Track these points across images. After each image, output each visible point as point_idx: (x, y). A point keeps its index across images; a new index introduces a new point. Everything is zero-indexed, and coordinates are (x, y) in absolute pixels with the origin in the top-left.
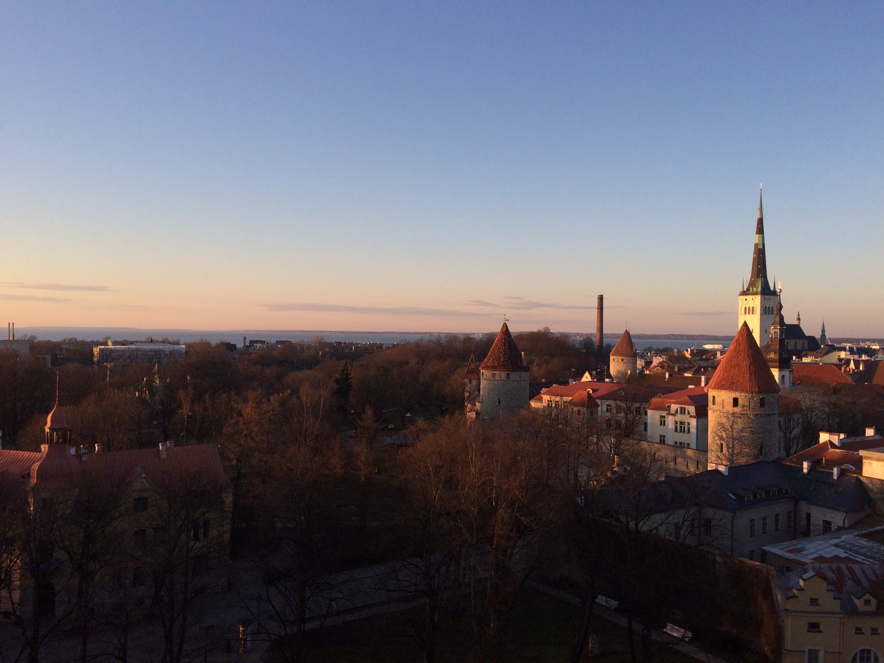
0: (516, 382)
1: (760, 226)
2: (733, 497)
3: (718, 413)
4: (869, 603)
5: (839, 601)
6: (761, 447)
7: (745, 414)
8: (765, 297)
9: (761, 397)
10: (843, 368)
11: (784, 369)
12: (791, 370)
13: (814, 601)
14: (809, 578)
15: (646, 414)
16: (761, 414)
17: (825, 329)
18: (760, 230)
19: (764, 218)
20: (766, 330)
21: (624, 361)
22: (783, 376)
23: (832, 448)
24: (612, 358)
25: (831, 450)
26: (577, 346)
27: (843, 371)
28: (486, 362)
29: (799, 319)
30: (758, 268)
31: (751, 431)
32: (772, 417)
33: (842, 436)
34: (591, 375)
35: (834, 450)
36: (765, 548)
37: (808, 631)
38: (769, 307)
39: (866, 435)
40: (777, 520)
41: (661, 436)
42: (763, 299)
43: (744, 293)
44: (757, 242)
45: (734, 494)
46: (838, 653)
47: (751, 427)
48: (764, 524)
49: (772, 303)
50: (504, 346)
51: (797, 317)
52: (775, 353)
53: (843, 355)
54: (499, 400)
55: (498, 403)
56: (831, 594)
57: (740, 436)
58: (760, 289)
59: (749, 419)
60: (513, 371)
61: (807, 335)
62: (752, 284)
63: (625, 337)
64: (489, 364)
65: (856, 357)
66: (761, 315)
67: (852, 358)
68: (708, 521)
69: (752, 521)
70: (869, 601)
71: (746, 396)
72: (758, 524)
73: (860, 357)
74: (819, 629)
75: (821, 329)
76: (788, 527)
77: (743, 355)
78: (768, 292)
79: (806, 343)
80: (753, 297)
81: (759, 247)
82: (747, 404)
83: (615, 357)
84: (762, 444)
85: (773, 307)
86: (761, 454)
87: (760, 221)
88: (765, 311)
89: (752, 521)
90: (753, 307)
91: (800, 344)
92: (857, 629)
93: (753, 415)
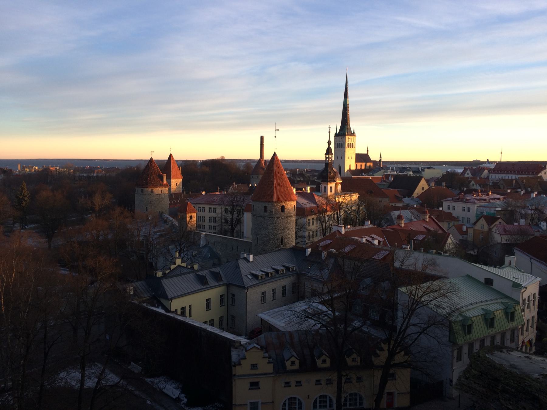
1: (346, 93)
2: (250, 278)
3: (256, 217)
4: (294, 364)
5: (272, 365)
6: (282, 239)
7: (271, 217)
9: (282, 205)
11: (331, 182)
12: (336, 183)
13: (254, 366)
14: (249, 350)
15: (243, 214)
17: (382, 156)
18: (346, 96)
20: (349, 157)
21: (259, 178)
22: (331, 187)
24: (251, 176)
26: (242, 168)
29: (368, 151)
34: (235, 188)
37: (249, 389)
38: (351, 144)
40: (284, 291)
46: (270, 402)
55: (146, 210)
56: (266, 360)
57: (268, 232)
59: (274, 220)
68: (233, 295)
69: (264, 293)
70: (294, 362)
71: (272, 205)
72: (269, 296)
74: (258, 386)
76: (293, 294)
80: (342, 137)
85: (353, 144)
86: (282, 244)
89: (264, 293)
90: (342, 143)
92: (286, 383)
93: (276, 217)
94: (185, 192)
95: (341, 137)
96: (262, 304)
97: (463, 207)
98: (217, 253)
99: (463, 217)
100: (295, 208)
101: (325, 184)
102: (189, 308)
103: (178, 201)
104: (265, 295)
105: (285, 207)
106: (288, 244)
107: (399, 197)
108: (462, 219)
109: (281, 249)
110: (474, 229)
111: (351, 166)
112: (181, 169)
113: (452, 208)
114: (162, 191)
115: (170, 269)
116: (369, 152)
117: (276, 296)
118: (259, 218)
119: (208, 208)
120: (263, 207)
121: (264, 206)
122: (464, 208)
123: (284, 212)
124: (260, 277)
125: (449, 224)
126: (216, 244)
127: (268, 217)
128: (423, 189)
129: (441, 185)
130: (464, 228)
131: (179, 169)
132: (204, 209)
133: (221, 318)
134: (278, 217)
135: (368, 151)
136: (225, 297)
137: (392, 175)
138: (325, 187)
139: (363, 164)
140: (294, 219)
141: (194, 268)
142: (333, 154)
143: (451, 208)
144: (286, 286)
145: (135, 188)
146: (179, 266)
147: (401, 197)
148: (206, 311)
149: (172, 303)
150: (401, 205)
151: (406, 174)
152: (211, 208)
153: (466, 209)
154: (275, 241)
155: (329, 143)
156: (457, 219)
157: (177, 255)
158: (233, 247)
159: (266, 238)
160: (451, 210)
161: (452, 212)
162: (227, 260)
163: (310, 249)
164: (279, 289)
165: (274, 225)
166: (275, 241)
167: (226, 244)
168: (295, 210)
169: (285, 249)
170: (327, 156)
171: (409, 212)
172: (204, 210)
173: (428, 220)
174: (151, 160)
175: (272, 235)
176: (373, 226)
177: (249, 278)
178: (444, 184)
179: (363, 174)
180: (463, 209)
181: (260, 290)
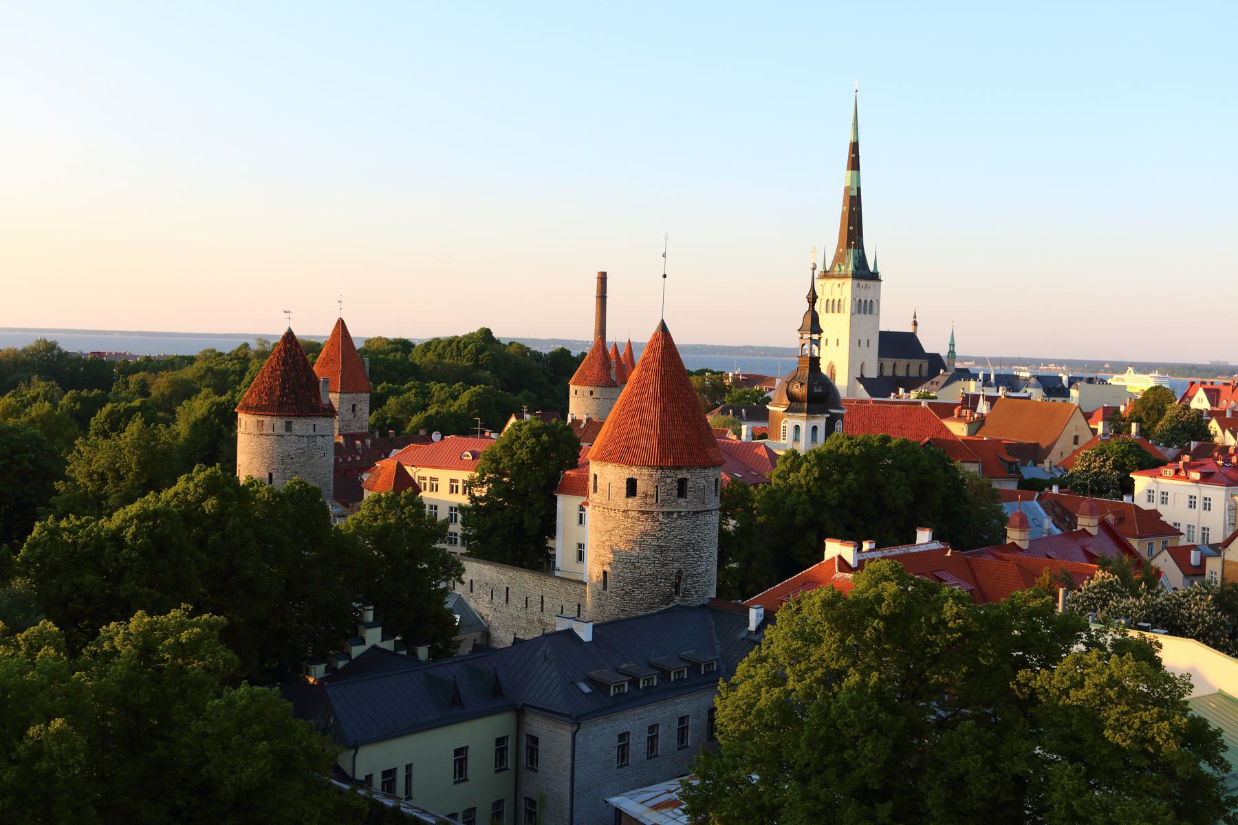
0: (305, 439)
1: (853, 156)
8: (859, 282)
9: (680, 476)
10: (956, 411)
16: (680, 512)
18: (854, 164)
19: (859, 141)
21: (593, 396)
22: (815, 428)
23: (840, 570)
24: (572, 388)
25: (838, 575)
27: (956, 416)
28: (245, 398)
29: (915, 324)
30: (849, 231)
31: (659, 546)
32: (701, 518)
33: (866, 546)
35: (843, 574)
36: (615, 801)
38: (866, 301)
39: (917, 543)
40: (682, 732)
41: (580, 546)
42: (855, 286)
43: (826, 275)
44: (849, 185)
45: (590, 681)
47: (658, 539)
48: (652, 741)
49: (866, 295)
50: (283, 365)
51: (912, 319)
52: (802, 384)
53: (972, 387)
54: (271, 475)
58: (851, 269)
60: (299, 416)
61: (926, 352)
62: (839, 259)
63: (597, 349)
64: (250, 402)
65: (991, 392)
66: (852, 314)
67: (982, 393)
68: (535, 740)
69: (623, 736)
72: (638, 745)
73: (998, 391)
75: (949, 342)
76: (708, 740)
77: (651, 391)
78: (864, 274)
79: (925, 364)
80: (840, 281)
81: (851, 194)
82: (651, 491)
83: (577, 387)
84: (680, 571)
85: (871, 301)
86: (677, 593)
87: (855, 147)
88: (860, 305)
89: (623, 736)
90: (840, 300)
91: (915, 367)
94: (377, 433)
95: (837, 282)
96: (618, 767)
97: (1191, 497)
98: (480, 614)
99: (1189, 526)
100: (719, 487)
101: (796, 418)
102: (407, 772)
103: (358, 458)
104: (628, 744)
105: (691, 483)
106: (696, 592)
107: (1010, 464)
108: (1189, 531)
109: (673, 607)
110: (1224, 561)
111: (911, 366)
112: (367, 365)
113: (1159, 503)
114: (317, 427)
115: (350, 657)
116: (918, 327)
117: (659, 747)
118: (613, 514)
119: (449, 481)
120: (626, 481)
121: (628, 480)
122: (1193, 500)
123: (686, 498)
124: (614, 687)
125: (1151, 544)
126: (475, 587)
127: (640, 511)
128: (1076, 438)
129: (1129, 432)
130: (1194, 558)
131: (364, 365)
132: (435, 483)
133: (498, 805)
134: (667, 512)
135: (915, 324)
136: (511, 744)
137: (988, 399)
138: (797, 427)
139: (902, 363)
140: (715, 518)
141: (417, 655)
142: (822, 331)
143: (1158, 497)
144: (688, 716)
145: (239, 414)
146: (374, 647)
147: (1015, 463)
148: (455, 783)
149: (357, 756)
150: (1012, 486)
151: (1026, 395)
152: (456, 481)
153: (1200, 503)
154: (657, 585)
155: (813, 298)
156: (1174, 531)
157: (369, 616)
158: (527, 598)
159: (630, 575)
160: (1155, 505)
161: (1162, 509)
162: (515, 634)
163: (763, 609)
164: (669, 726)
165: (654, 536)
166: (657, 585)
167: (507, 588)
168: (719, 494)
169: (688, 608)
170: (807, 336)
171: (1040, 509)
172: (437, 486)
173: (1094, 531)
174: (290, 335)
175: (650, 564)
176: (943, 547)
177: (581, 691)
178: (1134, 425)
179: (901, 390)
180: (1191, 502)
181: (612, 727)
